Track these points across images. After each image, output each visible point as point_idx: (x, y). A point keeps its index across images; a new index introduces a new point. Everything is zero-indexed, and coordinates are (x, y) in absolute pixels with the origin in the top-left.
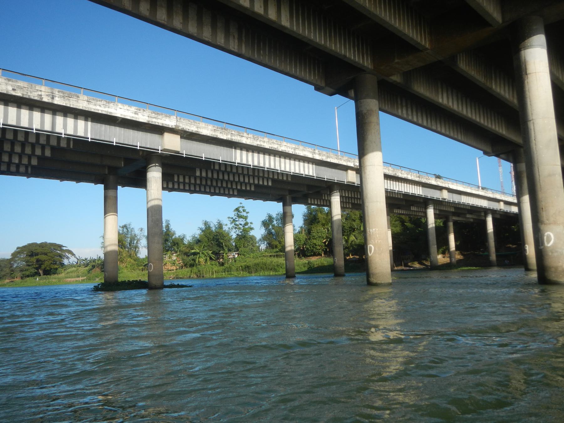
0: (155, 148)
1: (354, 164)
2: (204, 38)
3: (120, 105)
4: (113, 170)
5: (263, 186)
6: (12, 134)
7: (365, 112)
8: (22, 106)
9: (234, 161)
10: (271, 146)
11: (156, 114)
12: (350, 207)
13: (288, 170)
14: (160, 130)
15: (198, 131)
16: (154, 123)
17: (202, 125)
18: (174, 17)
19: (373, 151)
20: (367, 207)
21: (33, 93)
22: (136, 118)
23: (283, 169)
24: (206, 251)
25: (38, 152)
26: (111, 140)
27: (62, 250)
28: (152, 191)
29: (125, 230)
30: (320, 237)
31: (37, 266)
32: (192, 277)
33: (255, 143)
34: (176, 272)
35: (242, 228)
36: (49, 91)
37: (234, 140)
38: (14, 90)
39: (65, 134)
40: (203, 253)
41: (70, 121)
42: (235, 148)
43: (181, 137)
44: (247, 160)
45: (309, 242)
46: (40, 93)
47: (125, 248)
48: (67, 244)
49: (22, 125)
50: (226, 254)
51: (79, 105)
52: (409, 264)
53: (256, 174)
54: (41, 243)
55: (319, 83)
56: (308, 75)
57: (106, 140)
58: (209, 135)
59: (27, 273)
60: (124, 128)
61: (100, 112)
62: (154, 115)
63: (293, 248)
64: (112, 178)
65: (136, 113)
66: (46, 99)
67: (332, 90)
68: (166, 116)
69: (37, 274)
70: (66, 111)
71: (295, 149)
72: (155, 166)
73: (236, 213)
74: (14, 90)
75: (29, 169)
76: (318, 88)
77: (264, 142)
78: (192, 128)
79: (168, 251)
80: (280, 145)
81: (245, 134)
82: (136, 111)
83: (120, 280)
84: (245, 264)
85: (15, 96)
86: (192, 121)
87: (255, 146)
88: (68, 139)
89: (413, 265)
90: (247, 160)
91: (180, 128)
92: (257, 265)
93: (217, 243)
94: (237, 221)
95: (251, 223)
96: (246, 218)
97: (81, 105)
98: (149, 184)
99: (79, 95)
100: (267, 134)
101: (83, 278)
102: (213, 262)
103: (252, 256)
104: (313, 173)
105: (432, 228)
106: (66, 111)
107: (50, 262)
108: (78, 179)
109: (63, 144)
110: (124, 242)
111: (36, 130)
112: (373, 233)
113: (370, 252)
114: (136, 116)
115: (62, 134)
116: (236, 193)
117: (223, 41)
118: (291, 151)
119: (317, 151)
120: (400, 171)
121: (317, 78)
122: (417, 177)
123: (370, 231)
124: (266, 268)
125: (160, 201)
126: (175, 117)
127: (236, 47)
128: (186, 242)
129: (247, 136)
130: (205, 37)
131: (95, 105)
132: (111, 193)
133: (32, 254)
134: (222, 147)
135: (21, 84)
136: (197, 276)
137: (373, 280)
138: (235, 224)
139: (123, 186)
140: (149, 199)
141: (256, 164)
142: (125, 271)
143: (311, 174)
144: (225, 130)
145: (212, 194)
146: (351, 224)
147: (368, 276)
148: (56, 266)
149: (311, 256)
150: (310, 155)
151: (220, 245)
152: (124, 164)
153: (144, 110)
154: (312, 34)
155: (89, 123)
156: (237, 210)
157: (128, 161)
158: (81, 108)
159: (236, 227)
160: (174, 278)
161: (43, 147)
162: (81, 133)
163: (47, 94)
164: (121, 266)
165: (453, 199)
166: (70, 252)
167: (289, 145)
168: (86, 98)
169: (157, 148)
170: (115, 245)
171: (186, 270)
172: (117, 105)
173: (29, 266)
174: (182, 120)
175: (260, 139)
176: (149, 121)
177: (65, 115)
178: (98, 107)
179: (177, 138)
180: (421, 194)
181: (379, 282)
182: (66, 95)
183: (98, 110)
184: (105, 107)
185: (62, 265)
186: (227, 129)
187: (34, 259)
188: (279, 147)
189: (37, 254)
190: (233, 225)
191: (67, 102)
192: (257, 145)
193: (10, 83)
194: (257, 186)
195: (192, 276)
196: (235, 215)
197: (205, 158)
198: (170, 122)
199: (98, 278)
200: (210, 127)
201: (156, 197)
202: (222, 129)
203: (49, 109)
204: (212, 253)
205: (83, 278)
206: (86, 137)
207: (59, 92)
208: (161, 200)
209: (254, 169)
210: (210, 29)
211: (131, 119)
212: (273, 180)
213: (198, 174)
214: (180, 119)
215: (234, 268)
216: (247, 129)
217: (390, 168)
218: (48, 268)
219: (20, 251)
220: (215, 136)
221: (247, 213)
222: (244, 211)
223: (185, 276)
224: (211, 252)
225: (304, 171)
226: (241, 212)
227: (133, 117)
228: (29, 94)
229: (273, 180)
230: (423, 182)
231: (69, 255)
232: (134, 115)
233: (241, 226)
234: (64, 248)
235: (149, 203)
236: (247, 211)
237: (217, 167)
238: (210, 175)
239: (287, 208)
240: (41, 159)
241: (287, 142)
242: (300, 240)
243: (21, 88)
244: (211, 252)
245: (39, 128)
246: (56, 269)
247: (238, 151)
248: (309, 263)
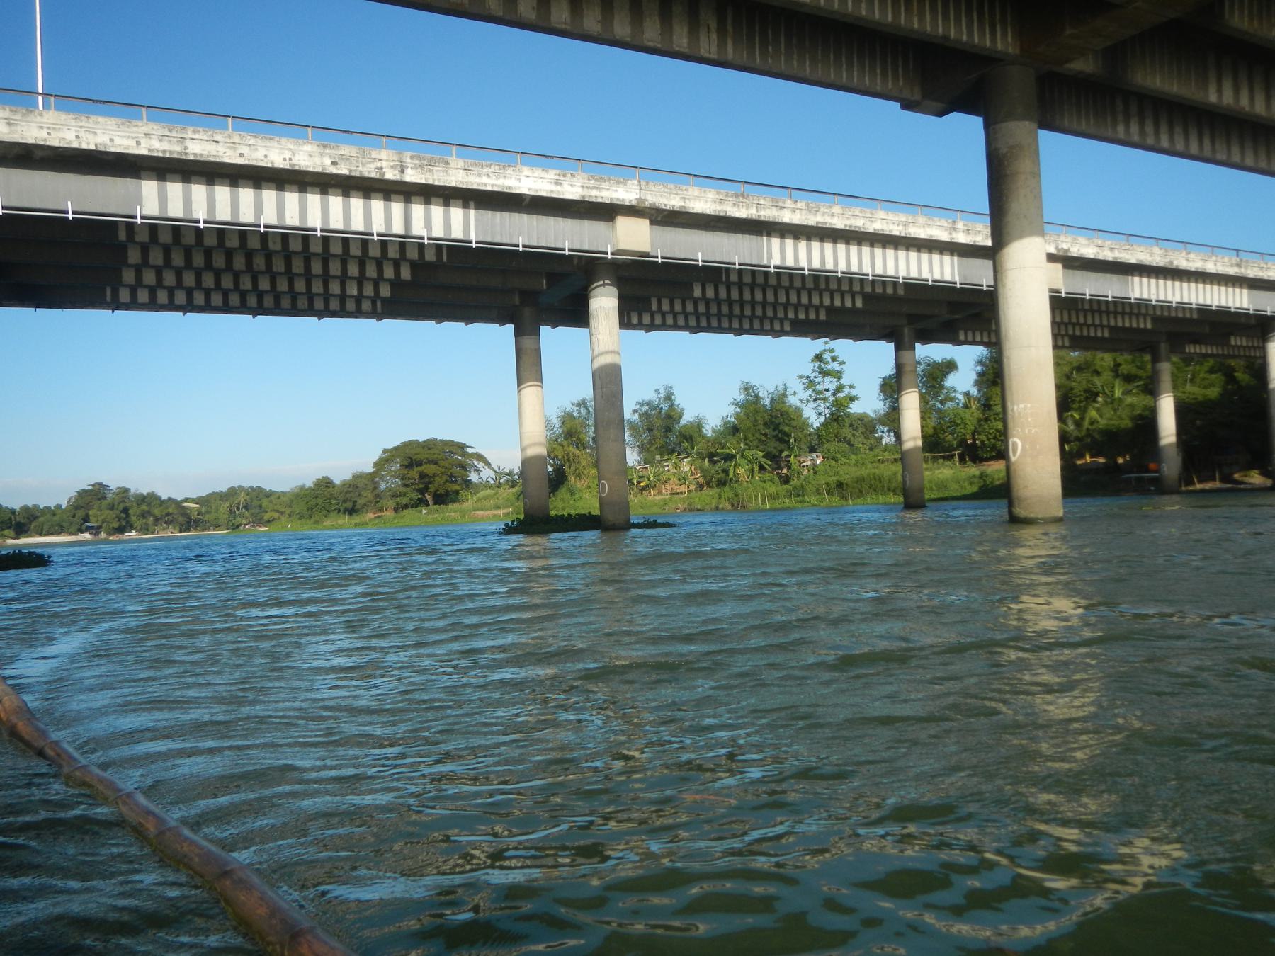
0: (600, 249)
1: (1057, 248)
2: (645, 42)
3: (526, 171)
4: (530, 297)
5: (843, 310)
6: (340, 244)
7: (1005, 150)
8: (352, 193)
9: (766, 262)
10: (848, 223)
11: (596, 180)
12: (1067, 344)
13: (891, 272)
14: (606, 212)
15: (684, 207)
16: (594, 200)
17: (694, 191)
18: (585, 12)
19: (1021, 237)
20: (1008, 358)
21: (368, 165)
22: (559, 192)
23: (879, 271)
24: (751, 452)
25: (389, 273)
26: (514, 242)
27: (464, 454)
28: (600, 337)
29: (583, 411)
31: (421, 486)
32: (723, 509)
33: (812, 220)
34: (688, 498)
35: (832, 399)
36: (395, 158)
37: (763, 218)
38: (334, 163)
39: (429, 239)
40: (743, 456)
41: (437, 211)
42: (769, 235)
43: (652, 223)
44: (796, 259)
45: (986, 427)
46: (379, 164)
47: (584, 448)
48: (476, 441)
49: (354, 228)
50: (795, 456)
51: (449, 178)
52: (1237, 476)
53: (823, 286)
54: (425, 442)
55: (906, 94)
56: (879, 81)
57: (505, 241)
58: (708, 212)
59: (405, 500)
60: (538, 213)
61: (489, 188)
62: (592, 182)
63: (919, 443)
64: (527, 312)
65: (557, 183)
66: (390, 175)
67: (940, 106)
68: (618, 182)
69: (422, 502)
70: (428, 193)
71: (906, 224)
72: (604, 285)
73: (817, 365)
74: (334, 163)
75: (379, 304)
76: (907, 105)
77: (833, 215)
78: (672, 201)
79: (673, 452)
80: (871, 219)
81: (789, 203)
82: (557, 177)
83: (553, 513)
84: (835, 479)
85: (337, 176)
86: (672, 186)
87: (812, 227)
88: (439, 247)
89: (1247, 480)
90: (796, 259)
91: (647, 204)
92: (860, 480)
94: (819, 383)
95: (851, 387)
96: (838, 375)
97: (453, 178)
98: (592, 322)
99: (451, 160)
100: (840, 198)
101: (506, 511)
102: (767, 476)
103: (853, 462)
104: (953, 274)
106: (428, 193)
107: (445, 477)
108: (469, 319)
109: (430, 256)
110: (582, 436)
111: (379, 235)
112: (1019, 413)
113: (1015, 452)
114: (559, 188)
115: (423, 238)
116: (787, 327)
117: (685, 42)
118: (896, 231)
119: (960, 225)
120: (1184, 254)
121: (901, 83)
122: (1232, 265)
123: (1013, 410)
124: (883, 487)
125: (617, 356)
126: (636, 182)
127: (714, 49)
128: (708, 432)
129: (793, 206)
130: (648, 41)
131: (479, 175)
132: (528, 342)
133: (410, 464)
134: (740, 235)
135: (346, 150)
136: (733, 505)
137: (1021, 512)
138: (814, 390)
139: (555, 325)
140: (596, 352)
141: (816, 264)
142: (587, 495)
143: (948, 277)
144: (743, 197)
145: (739, 332)
146: (1088, 382)
147: (1011, 505)
148: (457, 487)
149: (992, 458)
150: (943, 236)
151: (783, 438)
152: (547, 284)
153: (573, 176)
154: (863, 5)
155: (472, 212)
156: (819, 358)
157: (554, 278)
158: (453, 184)
159: (818, 397)
160: (685, 510)
161: (397, 265)
162: (457, 233)
163: (392, 164)
164: (579, 485)
166: (481, 458)
167: (891, 216)
168: (461, 163)
169: (604, 250)
170: (540, 444)
171: (710, 493)
172: (520, 171)
173: (406, 486)
174: (651, 186)
175: (822, 209)
176: (583, 197)
177: (427, 202)
178: (485, 180)
179: (643, 225)
180: (1245, 306)
181: (1032, 515)
182: (425, 162)
183: (486, 185)
184: (498, 178)
185: (468, 483)
186: (748, 196)
187: (414, 473)
188: (868, 223)
189: (419, 464)
190: (810, 392)
191: (428, 175)
192: (817, 223)
193: (327, 151)
194: (831, 310)
195: (721, 506)
196: (814, 371)
197: (703, 261)
198: (625, 193)
200: (711, 195)
201: (608, 348)
202: (737, 196)
203: (398, 192)
204: (764, 456)
205: (506, 511)
206: (467, 239)
207: (412, 157)
208: (619, 354)
209: (816, 278)
210: (658, 22)
211: (549, 195)
212: (867, 298)
213: (697, 292)
214: (647, 184)
215: (809, 488)
216: (794, 192)
217: (1156, 250)
218: (441, 491)
219: (389, 456)
220: (722, 214)
221: (842, 363)
222: (834, 359)
223: (708, 507)
224: (761, 454)
225: (931, 271)
226: (827, 363)
227: (552, 192)
228: (361, 168)
229: (867, 298)
230: (1251, 276)
231: (481, 465)
232: (553, 187)
233: (828, 394)
234: (469, 450)
235: (595, 361)
236: (840, 359)
237: (734, 278)
238: (723, 294)
239: (906, 355)
240: (396, 284)
241: (887, 210)
242: (966, 424)
243: (347, 159)
244: (761, 454)
245: (383, 230)
246: (457, 492)
247: (776, 241)
248: (982, 476)
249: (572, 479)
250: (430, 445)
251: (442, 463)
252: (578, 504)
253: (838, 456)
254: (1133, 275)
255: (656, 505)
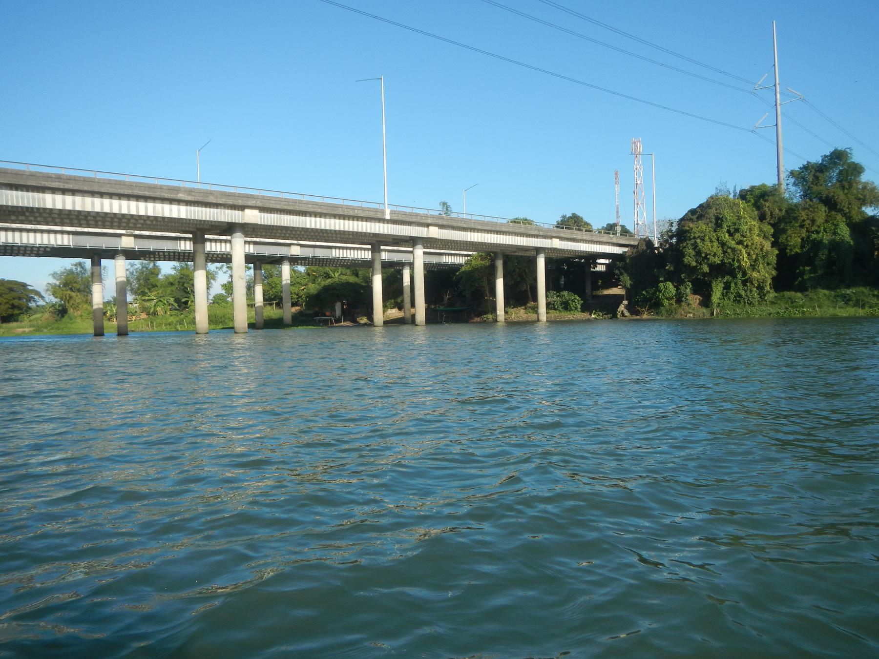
24: (166, 298)
29: (79, 269)
30: (298, 283)
40: (160, 301)
93: (183, 288)
102: (174, 312)
105: (286, 284)
107: (7, 306)
142: (79, 320)
143: (66, 243)
164: (76, 314)
165: (314, 254)
166: (38, 293)
199: (47, 328)
231: (36, 297)
234: (30, 288)
249: (71, 311)
250: (16, 283)
251: (6, 296)
252: (73, 325)
253: (220, 301)
254: (180, 240)
255: (113, 327)
